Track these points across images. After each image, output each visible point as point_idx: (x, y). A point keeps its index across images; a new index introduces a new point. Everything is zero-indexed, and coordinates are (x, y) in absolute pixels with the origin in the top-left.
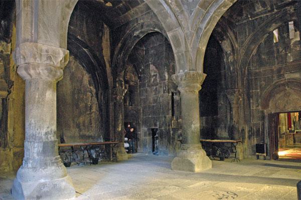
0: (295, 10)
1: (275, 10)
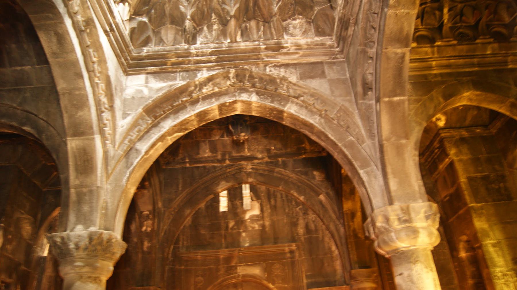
0: (252, 169)
1: (228, 162)
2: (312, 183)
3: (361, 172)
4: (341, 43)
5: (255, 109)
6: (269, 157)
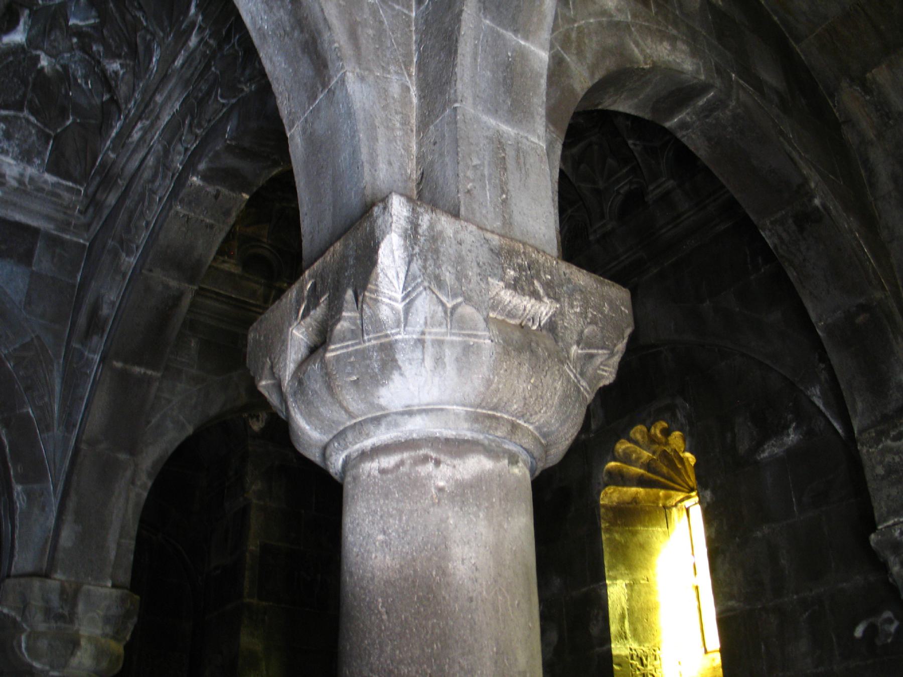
3: (18, 488)
4: (91, 210)
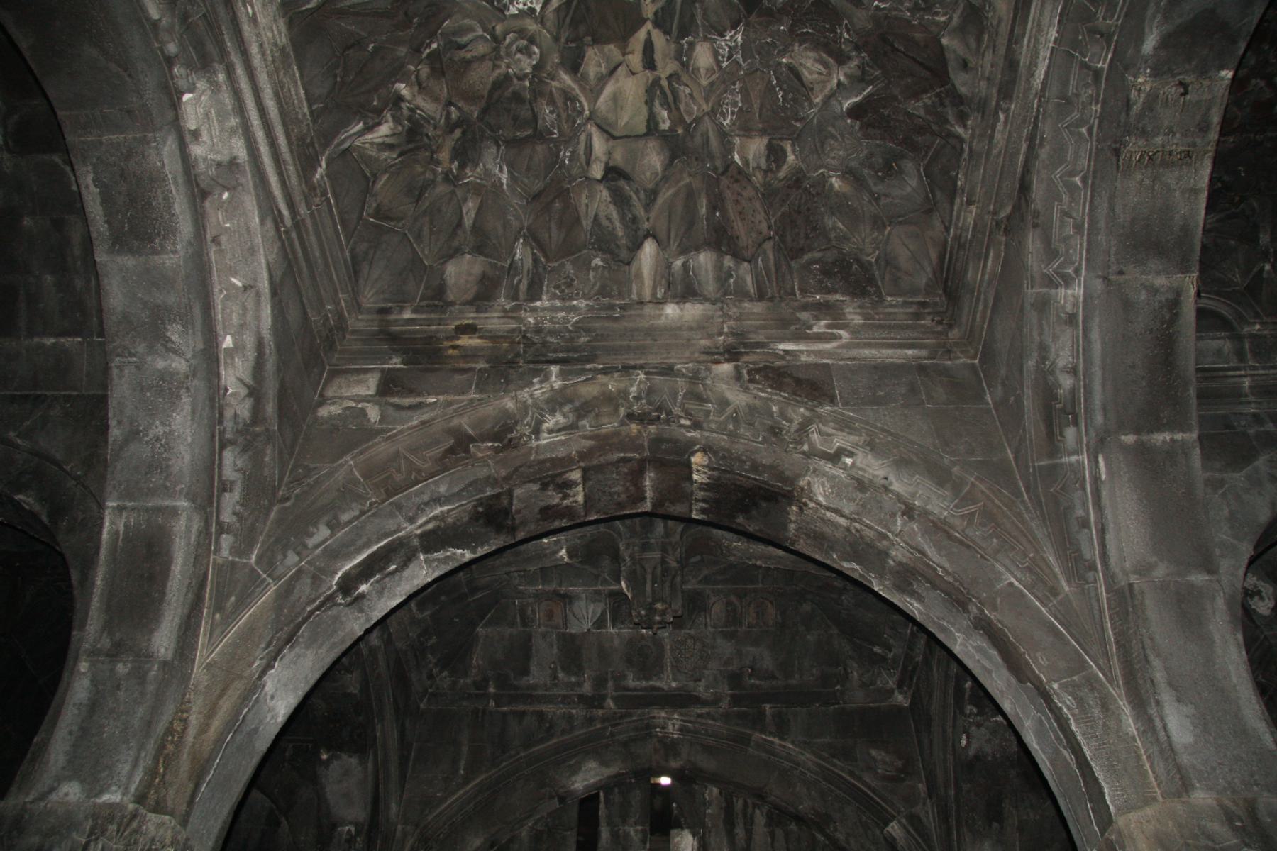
0: (681, 730)
1: (610, 703)
2: (865, 784)
5: (701, 494)
6: (736, 700)
